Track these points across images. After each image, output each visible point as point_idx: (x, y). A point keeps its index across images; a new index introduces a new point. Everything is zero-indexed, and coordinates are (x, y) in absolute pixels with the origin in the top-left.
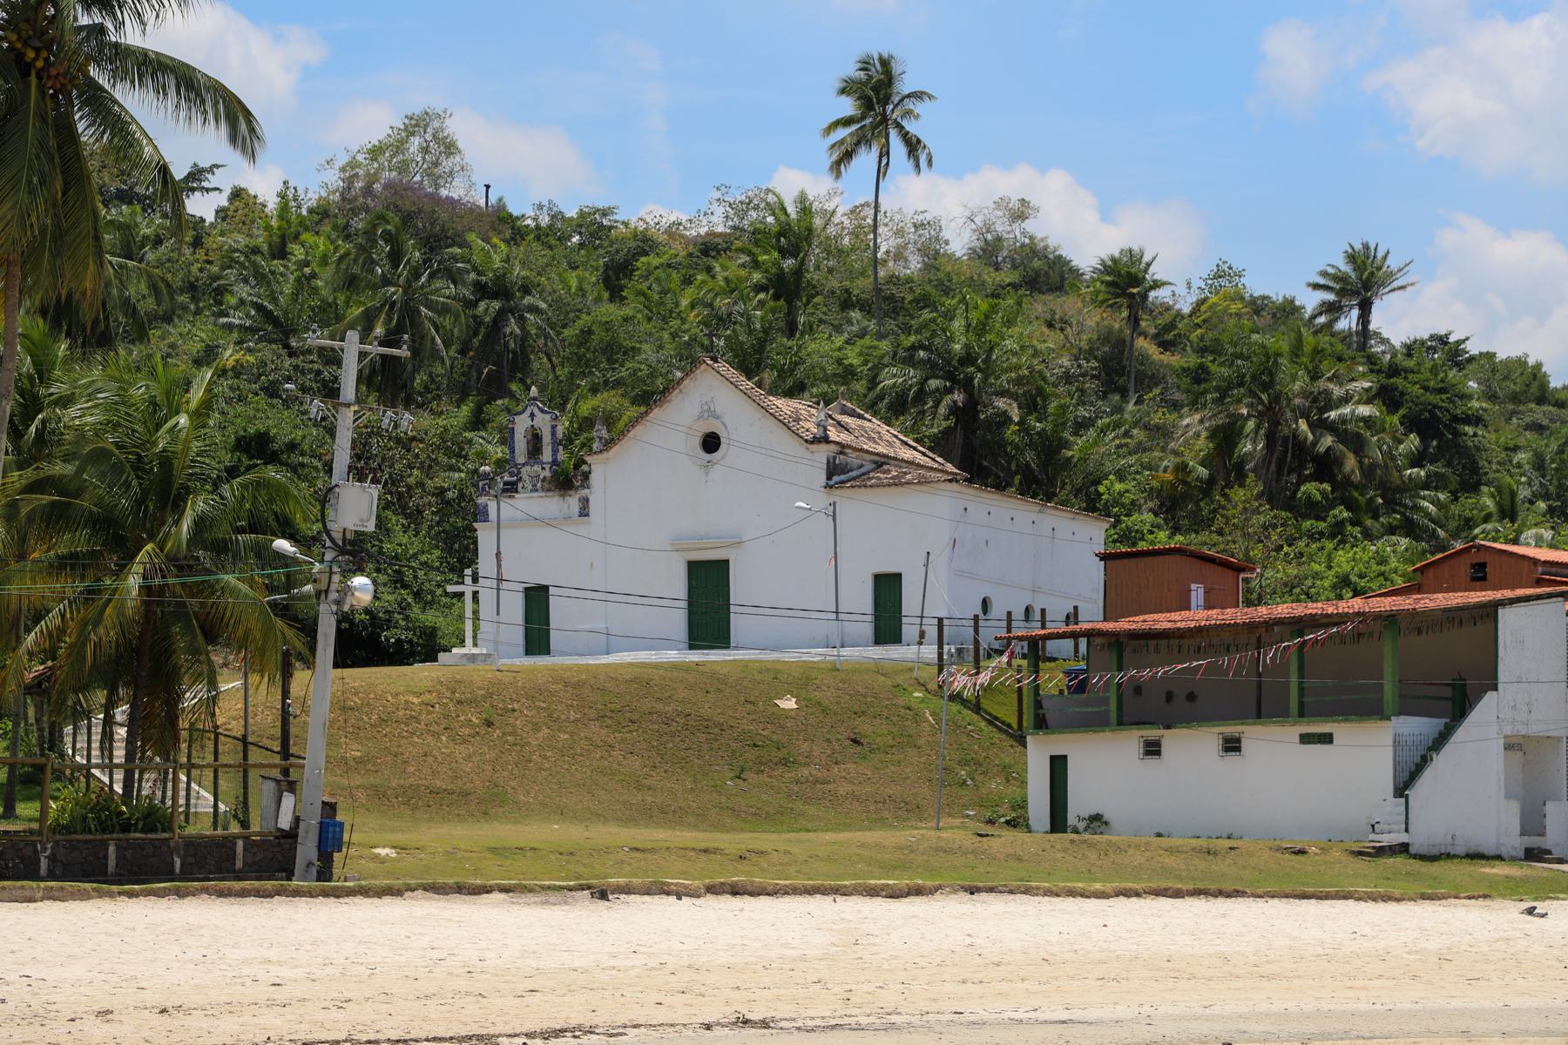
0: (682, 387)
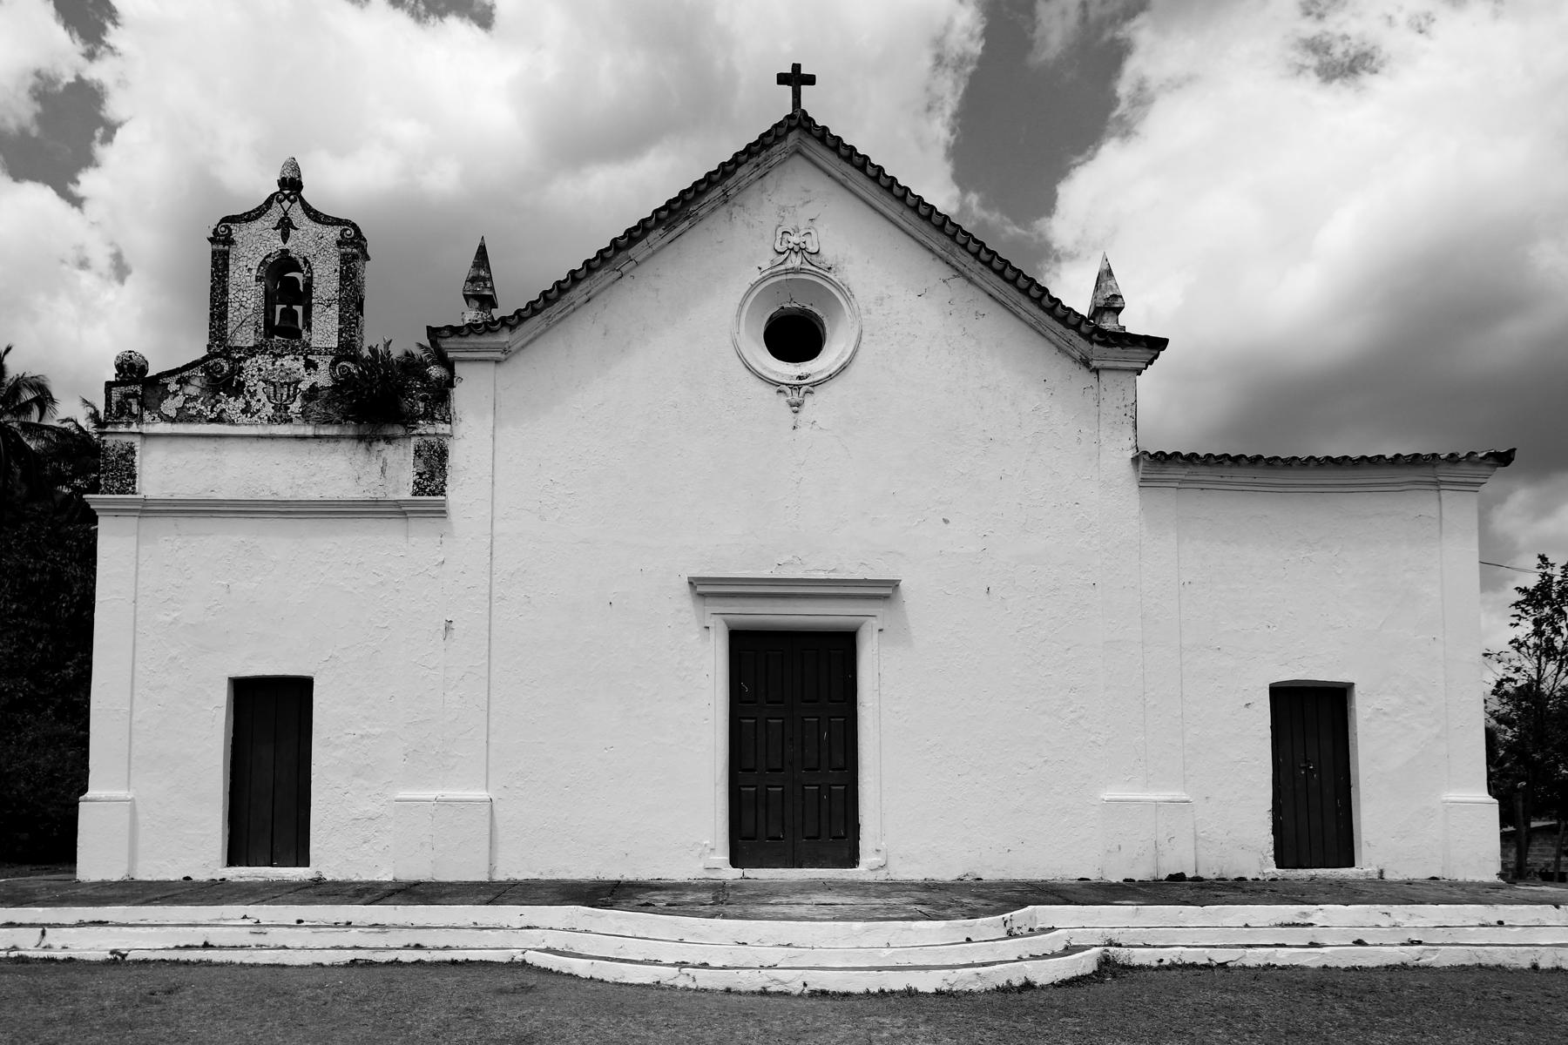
0: (730, 182)
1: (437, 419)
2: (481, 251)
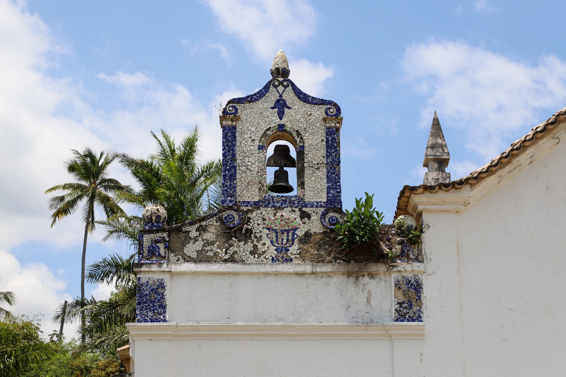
1: (411, 259)
2: (435, 123)
